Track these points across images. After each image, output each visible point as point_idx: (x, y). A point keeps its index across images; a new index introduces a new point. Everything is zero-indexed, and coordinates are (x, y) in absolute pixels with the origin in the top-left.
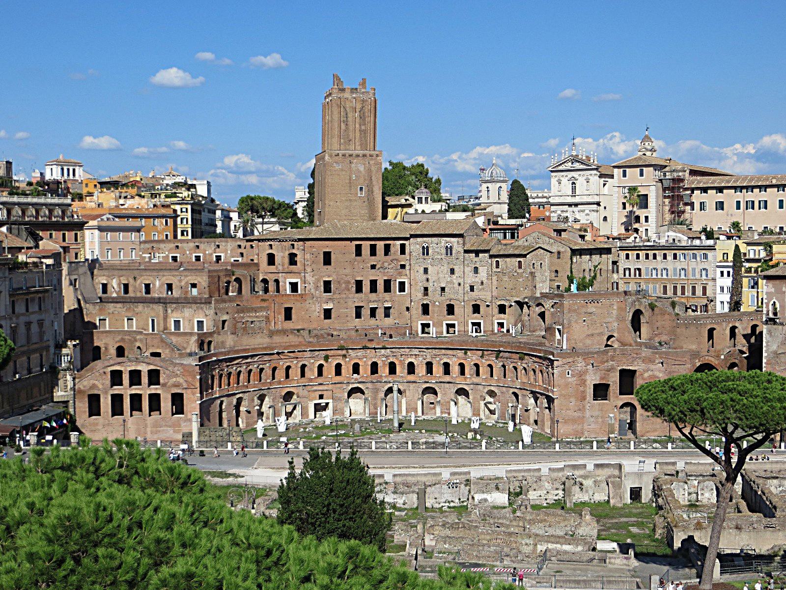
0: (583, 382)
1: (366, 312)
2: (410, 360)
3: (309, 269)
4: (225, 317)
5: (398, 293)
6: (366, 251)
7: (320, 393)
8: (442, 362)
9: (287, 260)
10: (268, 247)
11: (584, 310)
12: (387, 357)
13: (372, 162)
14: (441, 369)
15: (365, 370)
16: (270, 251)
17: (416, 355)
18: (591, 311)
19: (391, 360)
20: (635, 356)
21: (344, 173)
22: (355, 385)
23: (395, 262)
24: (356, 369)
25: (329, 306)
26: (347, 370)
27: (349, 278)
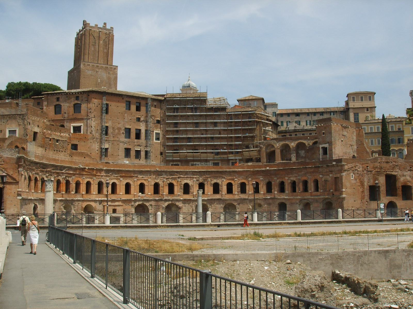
0: (362, 184)
1: (133, 153)
2: (186, 181)
3: (92, 115)
4: (37, 130)
5: (155, 141)
6: (133, 107)
7: (114, 208)
8: (213, 182)
9: (72, 110)
10: (55, 100)
11: (341, 133)
12: (167, 179)
13: (111, 72)
14: (211, 189)
15: (149, 190)
16: (57, 103)
17: (191, 177)
18: (345, 135)
19: (170, 181)
20: (394, 163)
21: (93, 77)
22: (141, 203)
23: (153, 117)
24: (142, 188)
25: (106, 146)
26: (134, 189)
27: (119, 126)
